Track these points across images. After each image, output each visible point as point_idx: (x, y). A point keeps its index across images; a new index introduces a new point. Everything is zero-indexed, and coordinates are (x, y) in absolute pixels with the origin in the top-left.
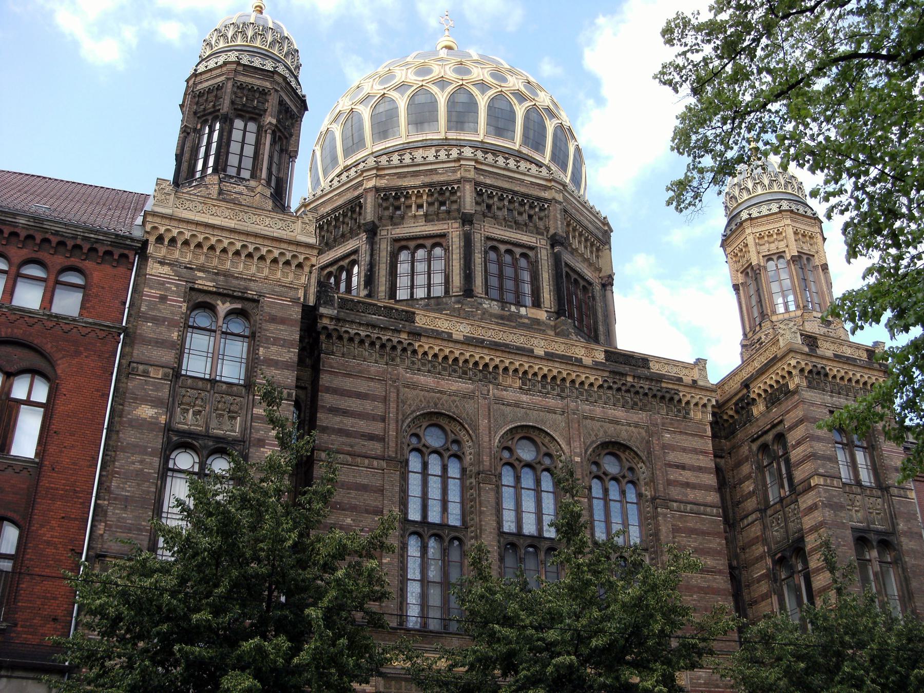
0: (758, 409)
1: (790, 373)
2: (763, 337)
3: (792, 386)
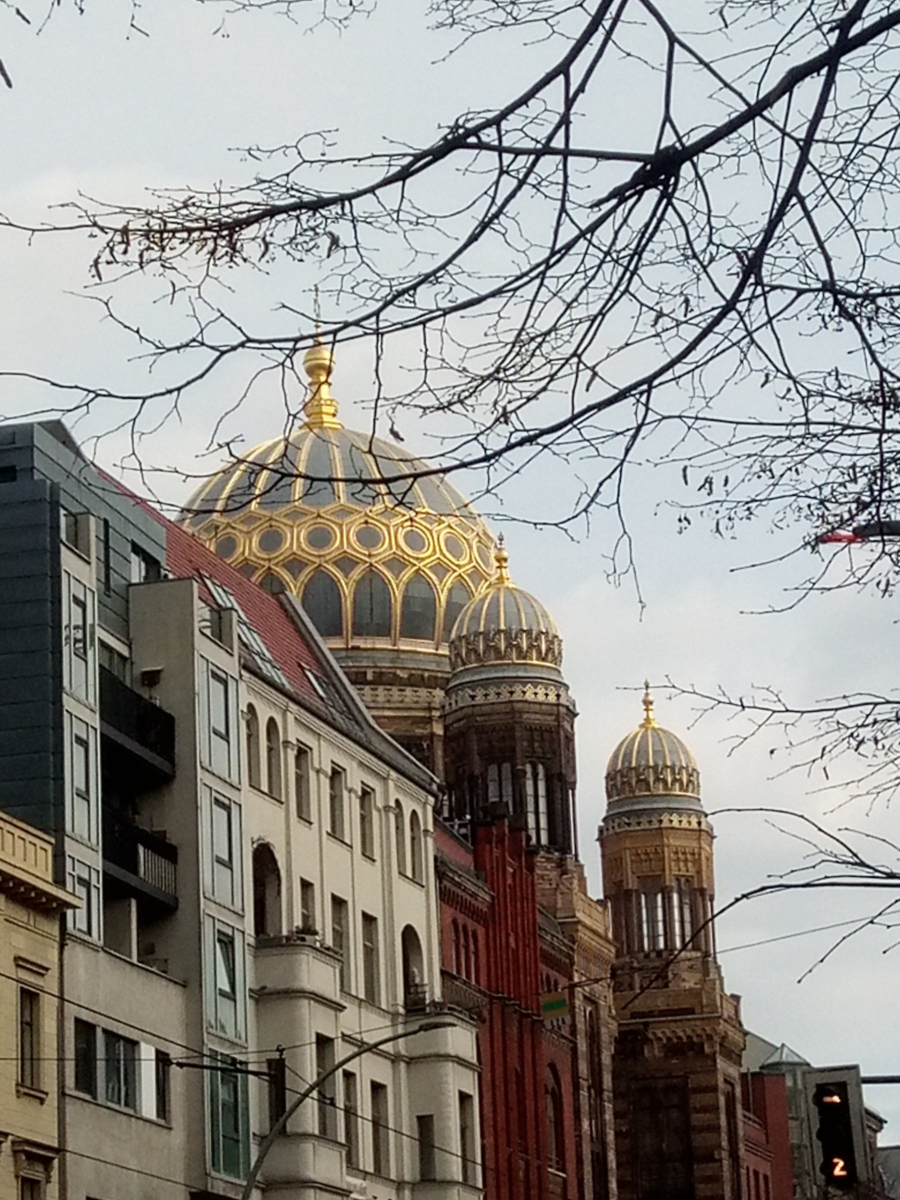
0: (653, 1052)
1: (710, 1037)
2: (670, 976)
3: (707, 1049)
